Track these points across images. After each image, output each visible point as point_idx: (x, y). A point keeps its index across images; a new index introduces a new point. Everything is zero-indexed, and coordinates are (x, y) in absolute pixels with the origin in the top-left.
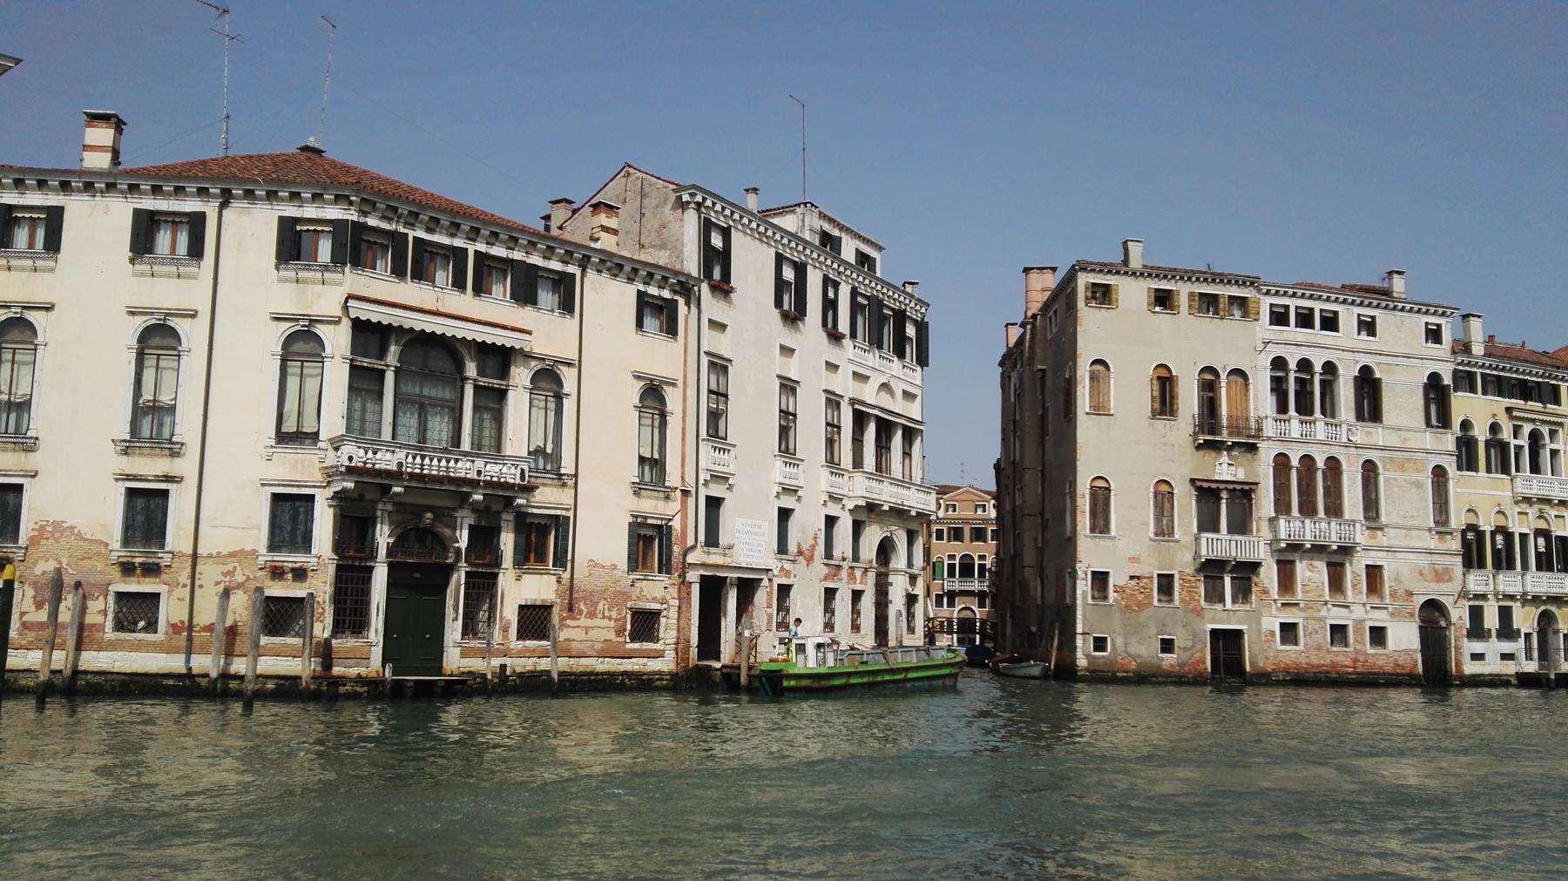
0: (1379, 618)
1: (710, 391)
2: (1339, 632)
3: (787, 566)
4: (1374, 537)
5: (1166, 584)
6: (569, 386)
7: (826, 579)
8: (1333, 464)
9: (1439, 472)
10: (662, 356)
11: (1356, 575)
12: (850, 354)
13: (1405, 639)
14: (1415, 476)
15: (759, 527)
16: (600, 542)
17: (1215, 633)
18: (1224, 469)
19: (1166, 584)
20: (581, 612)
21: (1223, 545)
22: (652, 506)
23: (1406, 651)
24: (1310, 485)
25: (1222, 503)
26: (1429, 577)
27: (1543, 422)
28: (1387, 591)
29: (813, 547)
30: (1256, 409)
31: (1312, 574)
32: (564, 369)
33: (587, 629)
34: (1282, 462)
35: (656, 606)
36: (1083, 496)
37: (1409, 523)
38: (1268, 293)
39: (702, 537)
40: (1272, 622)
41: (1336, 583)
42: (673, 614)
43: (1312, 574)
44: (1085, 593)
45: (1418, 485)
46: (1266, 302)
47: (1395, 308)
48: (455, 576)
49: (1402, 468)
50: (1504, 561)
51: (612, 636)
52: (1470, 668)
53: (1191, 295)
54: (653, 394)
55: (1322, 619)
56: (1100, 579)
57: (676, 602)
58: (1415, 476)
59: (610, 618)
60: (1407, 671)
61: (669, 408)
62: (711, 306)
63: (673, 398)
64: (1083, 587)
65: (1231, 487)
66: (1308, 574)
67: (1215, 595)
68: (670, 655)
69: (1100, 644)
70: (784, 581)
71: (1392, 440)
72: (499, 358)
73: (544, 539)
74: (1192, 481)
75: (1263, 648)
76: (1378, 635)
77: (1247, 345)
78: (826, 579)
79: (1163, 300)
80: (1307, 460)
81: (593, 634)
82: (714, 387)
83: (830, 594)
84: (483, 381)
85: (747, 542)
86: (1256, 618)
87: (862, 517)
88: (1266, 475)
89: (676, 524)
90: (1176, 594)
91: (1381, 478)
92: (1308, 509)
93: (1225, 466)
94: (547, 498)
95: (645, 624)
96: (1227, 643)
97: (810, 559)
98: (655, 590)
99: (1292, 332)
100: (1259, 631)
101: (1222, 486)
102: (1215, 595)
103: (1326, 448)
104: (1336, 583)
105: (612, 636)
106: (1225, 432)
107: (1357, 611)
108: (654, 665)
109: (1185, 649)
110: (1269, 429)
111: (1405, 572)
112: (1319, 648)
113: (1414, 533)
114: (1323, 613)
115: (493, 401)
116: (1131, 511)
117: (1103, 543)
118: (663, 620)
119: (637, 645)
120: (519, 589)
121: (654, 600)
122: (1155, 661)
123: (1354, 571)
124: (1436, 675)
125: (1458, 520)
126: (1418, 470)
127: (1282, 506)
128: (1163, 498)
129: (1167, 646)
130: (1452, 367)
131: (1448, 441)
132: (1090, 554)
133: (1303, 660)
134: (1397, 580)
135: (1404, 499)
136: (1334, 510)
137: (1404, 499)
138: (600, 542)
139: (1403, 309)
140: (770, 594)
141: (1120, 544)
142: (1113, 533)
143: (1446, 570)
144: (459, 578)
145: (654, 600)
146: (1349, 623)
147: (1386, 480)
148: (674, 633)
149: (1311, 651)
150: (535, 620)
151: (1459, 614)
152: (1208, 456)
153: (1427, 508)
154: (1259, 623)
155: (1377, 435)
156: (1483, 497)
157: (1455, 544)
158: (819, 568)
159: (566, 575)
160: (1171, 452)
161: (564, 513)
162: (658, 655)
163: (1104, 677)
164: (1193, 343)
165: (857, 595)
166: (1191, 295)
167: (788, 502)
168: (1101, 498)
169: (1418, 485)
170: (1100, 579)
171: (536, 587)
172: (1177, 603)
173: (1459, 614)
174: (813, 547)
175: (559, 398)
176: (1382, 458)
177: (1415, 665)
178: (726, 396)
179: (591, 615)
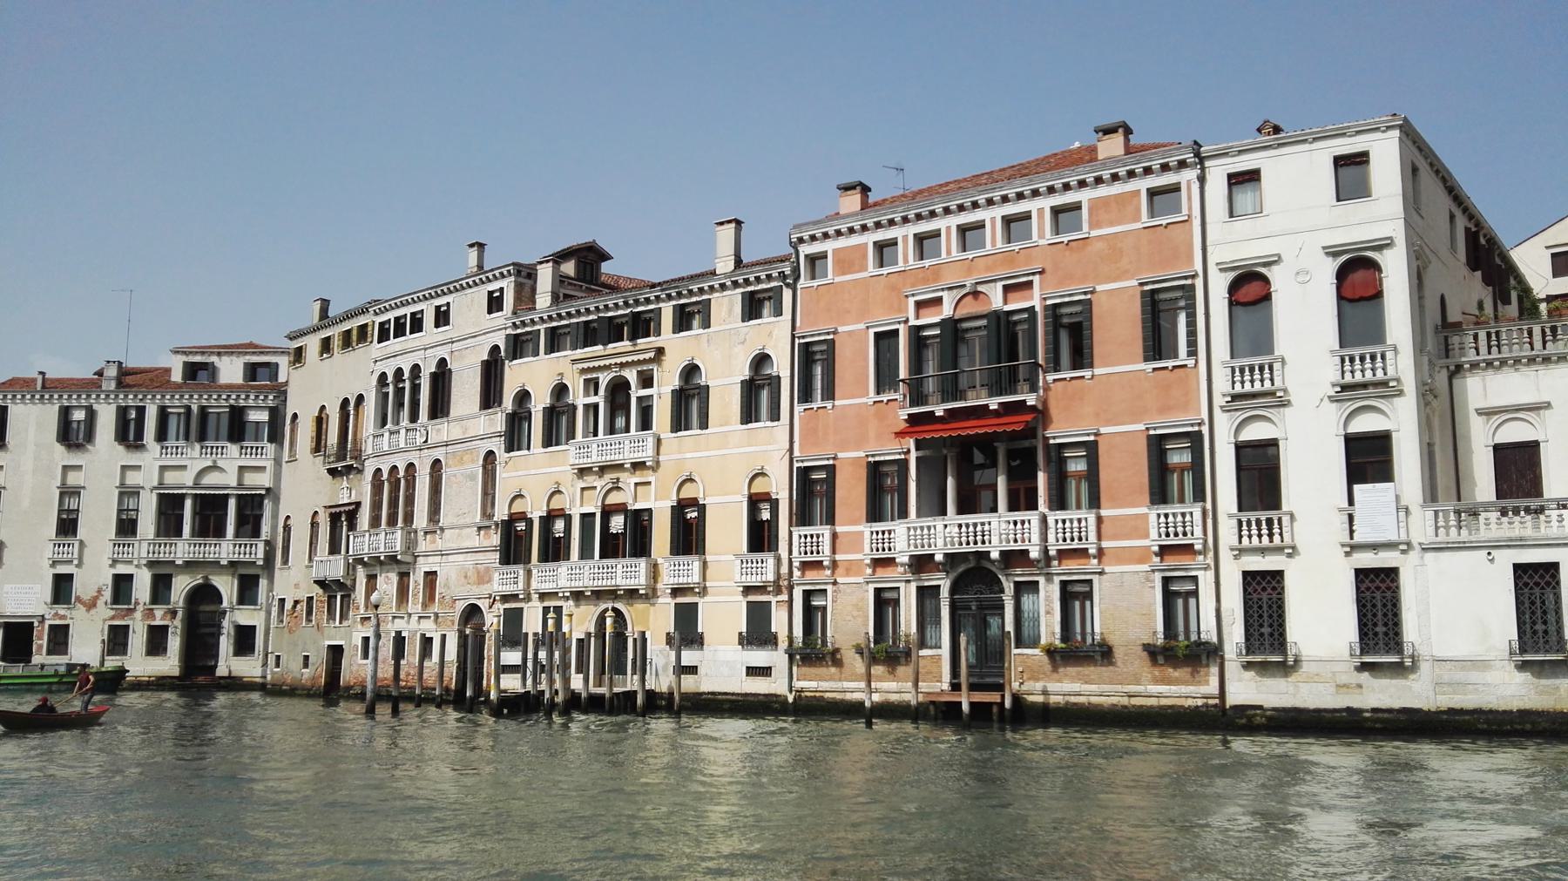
4: (434, 542)
7: (113, 618)
12: (151, 457)
24: (394, 493)
27: (622, 365)
29: (96, 599)
37: (462, 522)
45: (472, 478)
78: (113, 618)
79: (326, 345)
97: (91, 605)
110: (368, 449)
117: (285, 573)
123: (417, 579)
125: (501, 513)
127: (375, 522)
131: (497, 421)
134: (447, 586)
137: (462, 497)
151: (492, 620)
156: (541, 478)
173: (492, 620)
174: (96, 599)
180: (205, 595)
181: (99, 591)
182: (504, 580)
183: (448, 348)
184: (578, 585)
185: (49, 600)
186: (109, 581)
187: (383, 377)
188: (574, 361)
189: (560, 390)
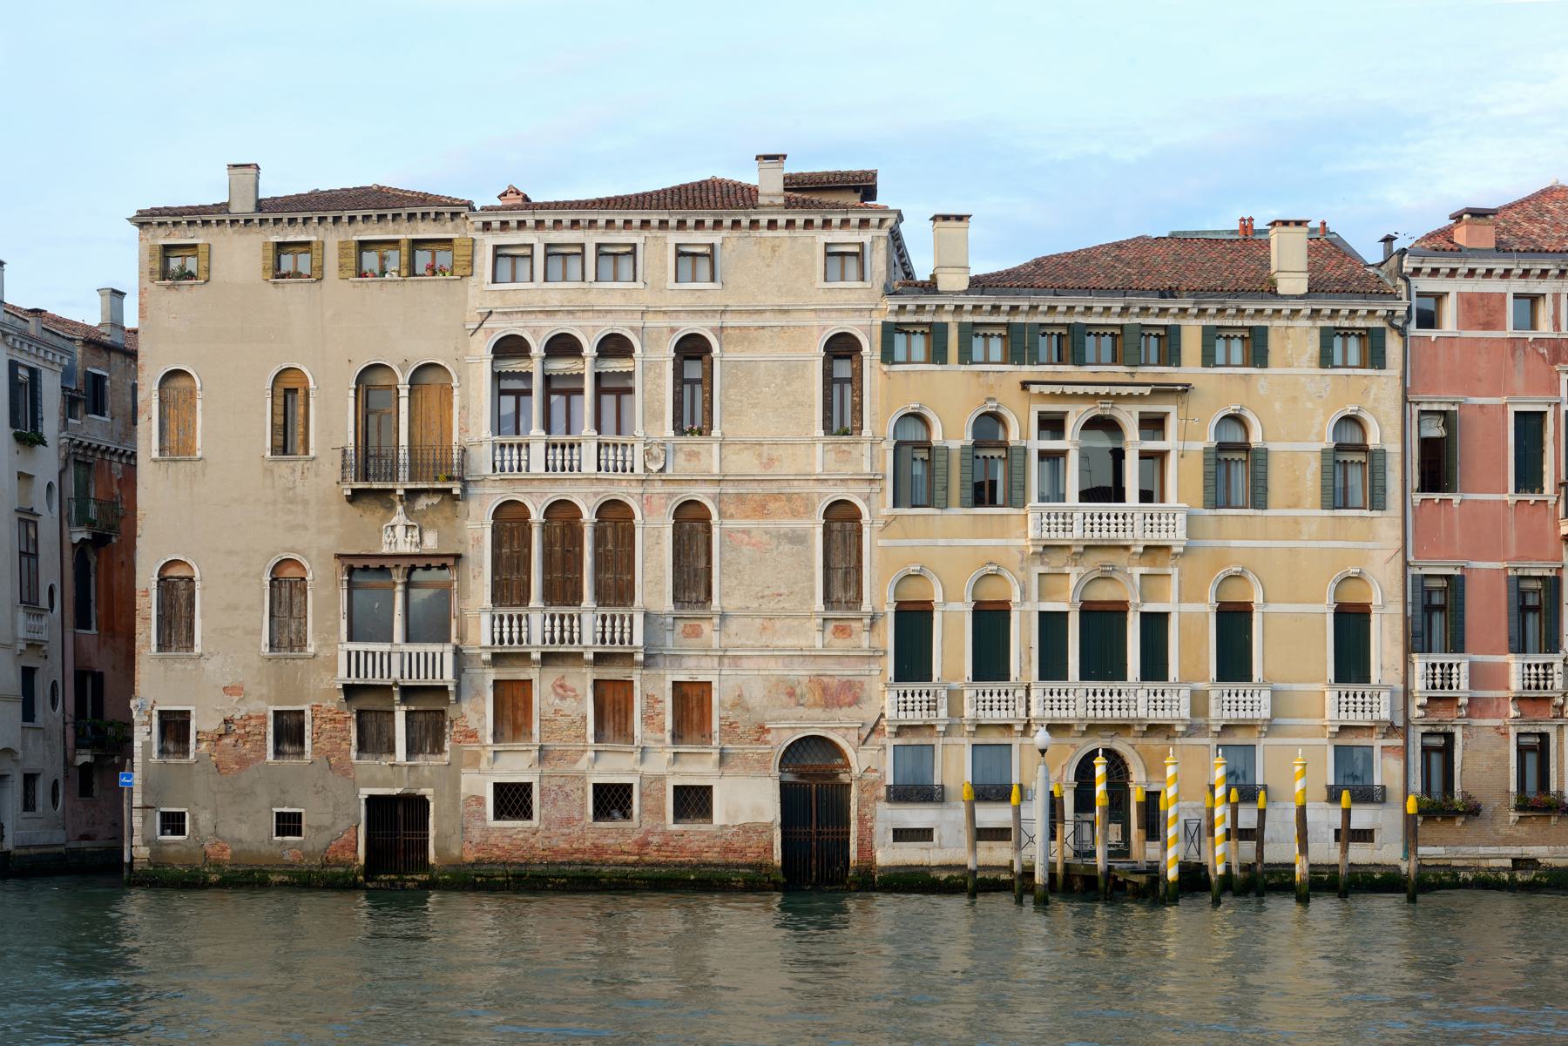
0: (696, 772)
2: (612, 800)
5: (289, 730)
8: (615, 515)
9: (842, 518)
14: (788, 524)
17: (372, 801)
24: (565, 555)
28: (715, 725)
30: (464, 430)
31: (562, 699)
34: (509, 518)
36: (147, 593)
38: (487, 226)
40: (480, 784)
41: (612, 709)
44: (147, 746)
46: (488, 242)
47: (754, 224)
52: (888, 855)
55: (581, 777)
58: (788, 524)
60: (751, 857)
67: (373, 739)
71: (743, 463)
74: (339, 556)
75: (463, 825)
76: (693, 801)
80: (562, 511)
88: (479, 540)
90: (308, 742)
91: (715, 531)
93: (400, 531)
96: (397, 820)
102: (373, 739)
104: (612, 709)
106: (403, 473)
107: (651, 762)
109: (319, 829)
110: (482, 461)
111: (756, 695)
113: (778, 624)
114: (583, 764)
116: (230, 614)
122: (265, 849)
123: (652, 692)
124: (814, 861)
126: (795, 514)
128: (286, 587)
129: (289, 824)
133: (539, 842)
134: (739, 703)
136: (616, 590)
139: (772, 224)
141: (210, 666)
142: (198, 650)
146: (634, 780)
149: (561, 827)
152: (368, 516)
153: (812, 578)
154: (462, 787)
155: (708, 457)
163: (174, 881)
168: (177, 595)
169: (797, 539)
170: (174, 727)
172: (308, 755)
173: (869, 764)
177: (769, 849)
184: (1060, 715)
187: (510, 347)
189: (989, 423)
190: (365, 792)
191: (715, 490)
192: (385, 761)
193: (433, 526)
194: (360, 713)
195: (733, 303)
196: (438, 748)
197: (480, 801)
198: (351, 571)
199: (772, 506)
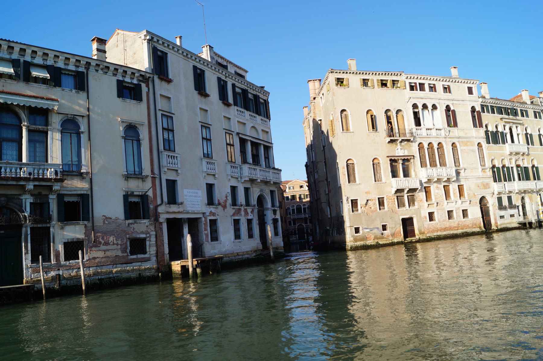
1: (164, 129)
3: (213, 210)
5: (381, 202)
6: (83, 128)
10: (136, 112)
11: (454, 190)
13: (475, 213)
14: (472, 148)
15: (197, 193)
16: (108, 206)
18: (399, 151)
19: (381, 202)
20: (100, 243)
21: (402, 182)
22: (135, 186)
23: (477, 218)
24: (433, 155)
25: (399, 166)
26: (481, 188)
27: (513, 123)
29: (226, 201)
32: (80, 119)
33: (105, 251)
35: (143, 236)
39: (165, 199)
42: (153, 239)
43: (437, 191)
46: (408, 81)
48: (24, 230)
49: (466, 145)
50: (509, 178)
51: (120, 253)
53: (378, 80)
54: (131, 131)
56: (354, 203)
57: (154, 233)
58: (472, 148)
59: (117, 244)
61: (141, 137)
62: (161, 87)
63: (144, 134)
64: (346, 207)
65: (403, 158)
66: (437, 191)
68: (154, 259)
69: (357, 230)
70: (212, 218)
71: (462, 134)
72: (40, 114)
73: (77, 209)
74: (388, 157)
76: (465, 213)
77: (402, 100)
78: (234, 215)
79: (365, 82)
81: (109, 254)
82: (165, 126)
83: (236, 222)
84: (33, 127)
85: (192, 201)
86: (418, 211)
87: (248, 185)
89: (150, 194)
92: (433, 164)
93: (399, 150)
94: (78, 185)
95: (138, 246)
96: (407, 223)
97: (225, 207)
98: (142, 227)
99: (418, 93)
100: (421, 216)
101: (399, 158)
102: (400, 204)
103: (438, 139)
105: (120, 253)
107: (456, 205)
108: (147, 265)
112: (444, 221)
115: (39, 138)
116: (363, 171)
118: (148, 243)
119: (135, 257)
120: (64, 233)
121: (142, 233)
128: (375, 166)
130: (479, 103)
132: (348, 192)
135: (469, 158)
138: (108, 206)
140: (205, 224)
143: (487, 184)
144: (26, 231)
145: (142, 233)
147: (461, 150)
148: (155, 248)
150: (73, 249)
152: (393, 145)
157: (490, 173)
158: (230, 210)
159: (89, 224)
160: (379, 147)
161: (85, 192)
162: (148, 260)
164: (381, 100)
165: (249, 222)
166: (378, 80)
167: (211, 181)
168: (350, 168)
169: (473, 151)
170: (354, 203)
171: (75, 232)
174: (226, 201)
175: (79, 134)
176: (459, 142)
177: (480, 223)
178: (173, 131)
179: (107, 244)
180: (261, 200)
181: (226, 197)
182: (496, 187)
183: (452, 102)
185: (206, 201)
186: (229, 190)
188: (501, 119)
190: (401, 217)
191: (458, 140)
192: (404, 209)
193: (406, 149)
194: (397, 197)
195: (456, 98)
196: (414, 204)
197: (426, 218)
198: (391, 160)
199: (468, 144)
